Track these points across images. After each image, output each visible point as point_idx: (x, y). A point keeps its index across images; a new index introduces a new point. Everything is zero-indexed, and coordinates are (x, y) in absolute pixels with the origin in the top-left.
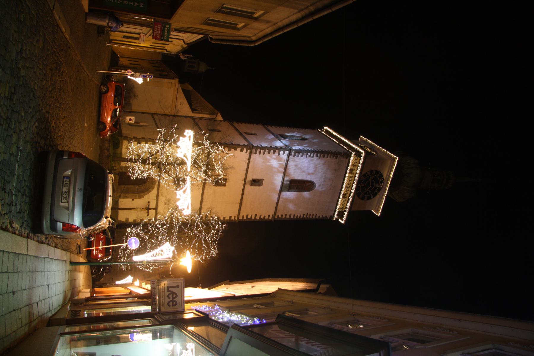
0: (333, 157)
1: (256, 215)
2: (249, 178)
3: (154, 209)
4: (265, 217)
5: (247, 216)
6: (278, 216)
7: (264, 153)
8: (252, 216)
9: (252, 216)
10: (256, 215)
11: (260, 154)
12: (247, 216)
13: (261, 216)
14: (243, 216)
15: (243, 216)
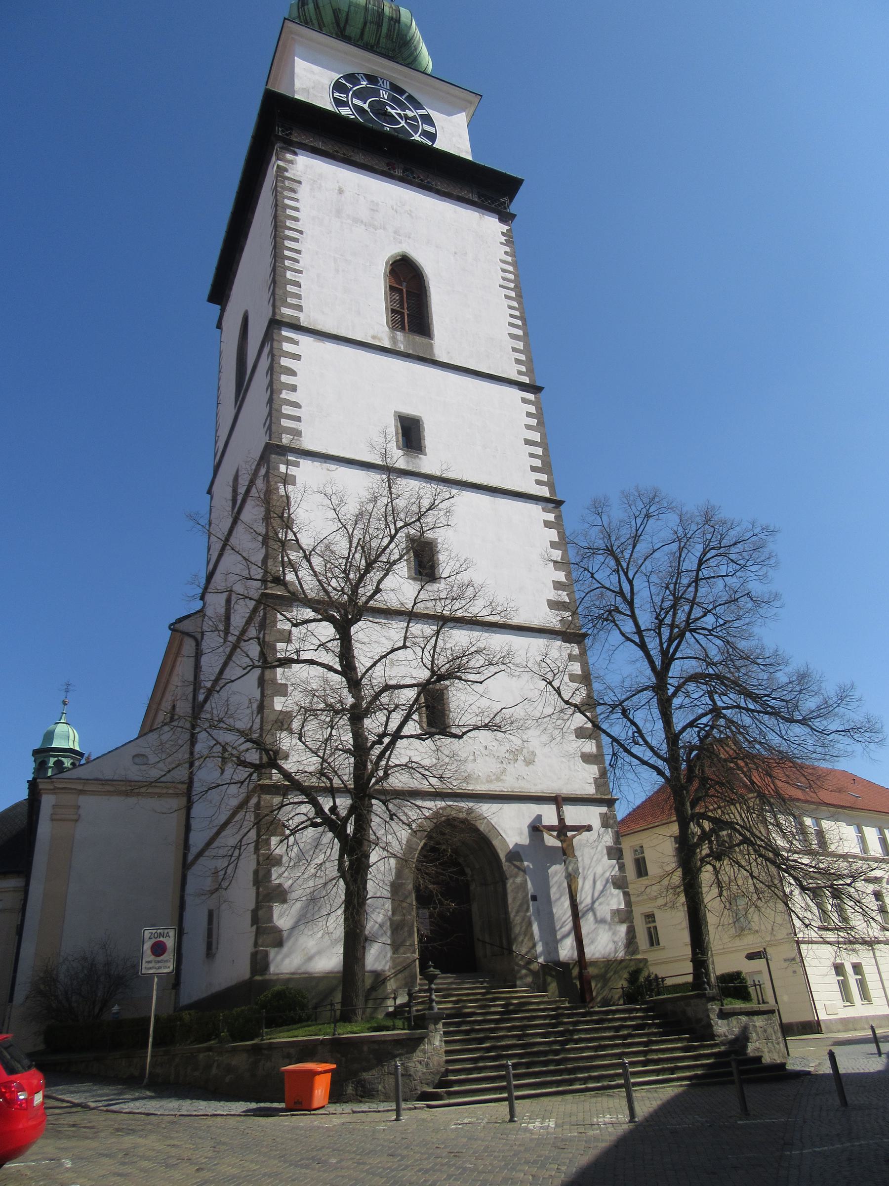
0: (294, 191)
1: (528, 442)
2: (399, 459)
3: (561, 819)
4: (529, 415)
5: (534, 469)
6: (520, 373)
7: (297, 405)
8: (532, 455)
9: (532, 455)
10: (528, 442)
11: (298, 419)
12: (534, 469)
13: (528, 427)
14: (538, 482)
15: (538, 482)
